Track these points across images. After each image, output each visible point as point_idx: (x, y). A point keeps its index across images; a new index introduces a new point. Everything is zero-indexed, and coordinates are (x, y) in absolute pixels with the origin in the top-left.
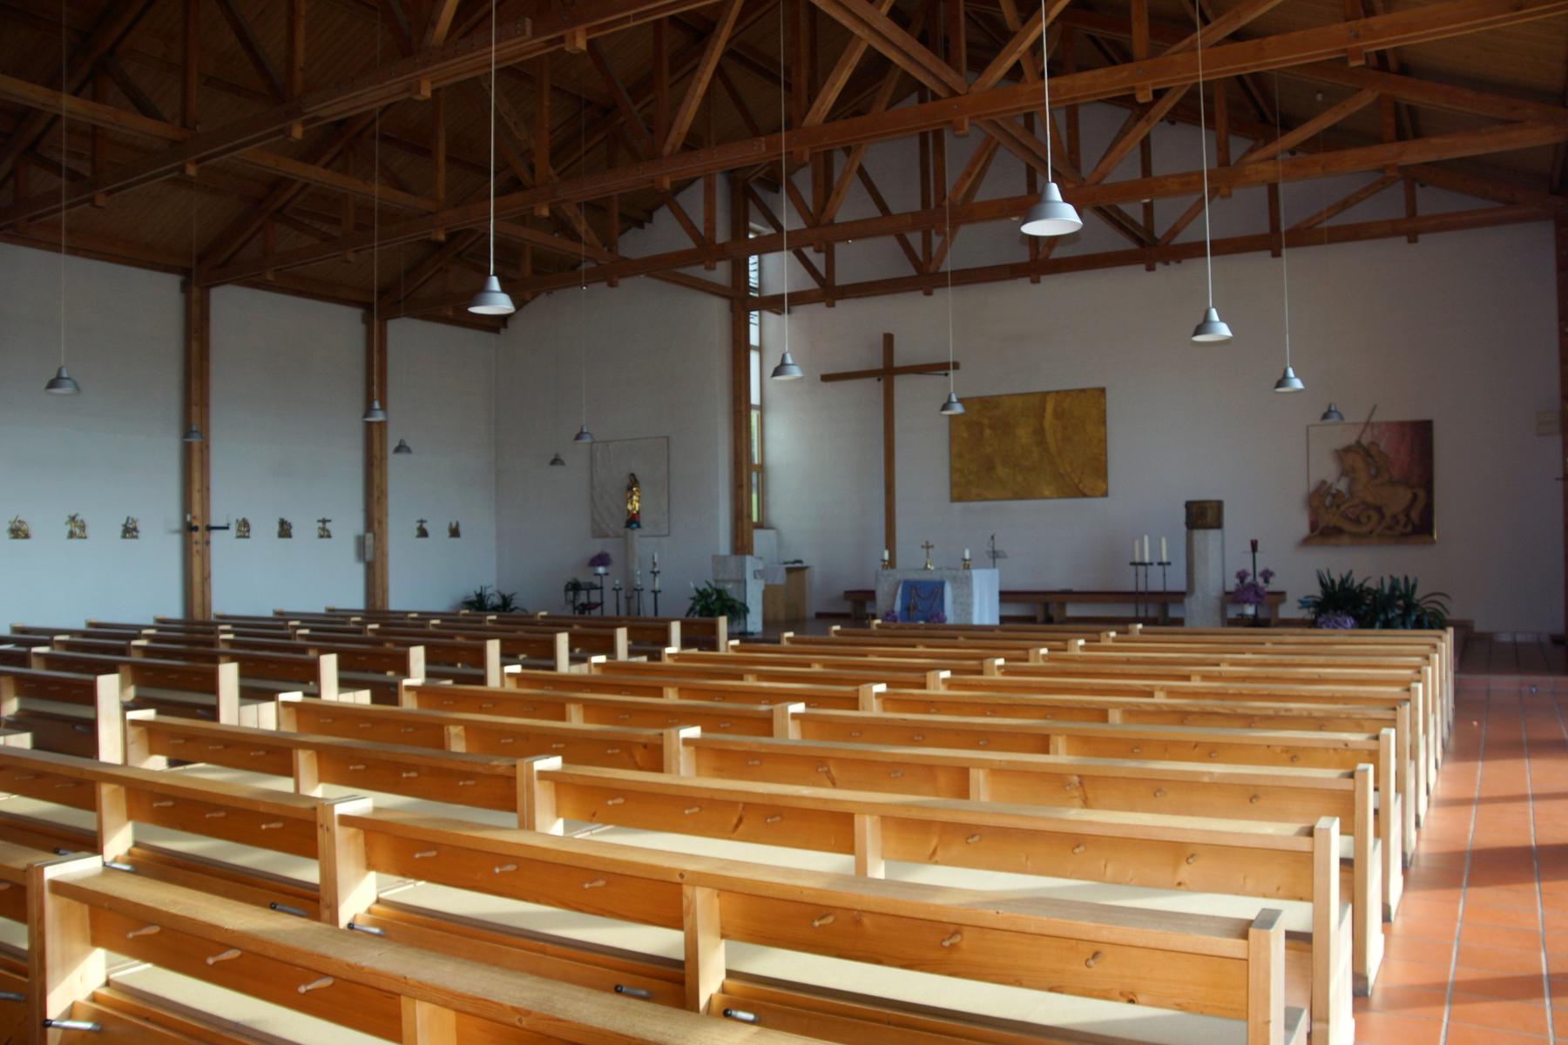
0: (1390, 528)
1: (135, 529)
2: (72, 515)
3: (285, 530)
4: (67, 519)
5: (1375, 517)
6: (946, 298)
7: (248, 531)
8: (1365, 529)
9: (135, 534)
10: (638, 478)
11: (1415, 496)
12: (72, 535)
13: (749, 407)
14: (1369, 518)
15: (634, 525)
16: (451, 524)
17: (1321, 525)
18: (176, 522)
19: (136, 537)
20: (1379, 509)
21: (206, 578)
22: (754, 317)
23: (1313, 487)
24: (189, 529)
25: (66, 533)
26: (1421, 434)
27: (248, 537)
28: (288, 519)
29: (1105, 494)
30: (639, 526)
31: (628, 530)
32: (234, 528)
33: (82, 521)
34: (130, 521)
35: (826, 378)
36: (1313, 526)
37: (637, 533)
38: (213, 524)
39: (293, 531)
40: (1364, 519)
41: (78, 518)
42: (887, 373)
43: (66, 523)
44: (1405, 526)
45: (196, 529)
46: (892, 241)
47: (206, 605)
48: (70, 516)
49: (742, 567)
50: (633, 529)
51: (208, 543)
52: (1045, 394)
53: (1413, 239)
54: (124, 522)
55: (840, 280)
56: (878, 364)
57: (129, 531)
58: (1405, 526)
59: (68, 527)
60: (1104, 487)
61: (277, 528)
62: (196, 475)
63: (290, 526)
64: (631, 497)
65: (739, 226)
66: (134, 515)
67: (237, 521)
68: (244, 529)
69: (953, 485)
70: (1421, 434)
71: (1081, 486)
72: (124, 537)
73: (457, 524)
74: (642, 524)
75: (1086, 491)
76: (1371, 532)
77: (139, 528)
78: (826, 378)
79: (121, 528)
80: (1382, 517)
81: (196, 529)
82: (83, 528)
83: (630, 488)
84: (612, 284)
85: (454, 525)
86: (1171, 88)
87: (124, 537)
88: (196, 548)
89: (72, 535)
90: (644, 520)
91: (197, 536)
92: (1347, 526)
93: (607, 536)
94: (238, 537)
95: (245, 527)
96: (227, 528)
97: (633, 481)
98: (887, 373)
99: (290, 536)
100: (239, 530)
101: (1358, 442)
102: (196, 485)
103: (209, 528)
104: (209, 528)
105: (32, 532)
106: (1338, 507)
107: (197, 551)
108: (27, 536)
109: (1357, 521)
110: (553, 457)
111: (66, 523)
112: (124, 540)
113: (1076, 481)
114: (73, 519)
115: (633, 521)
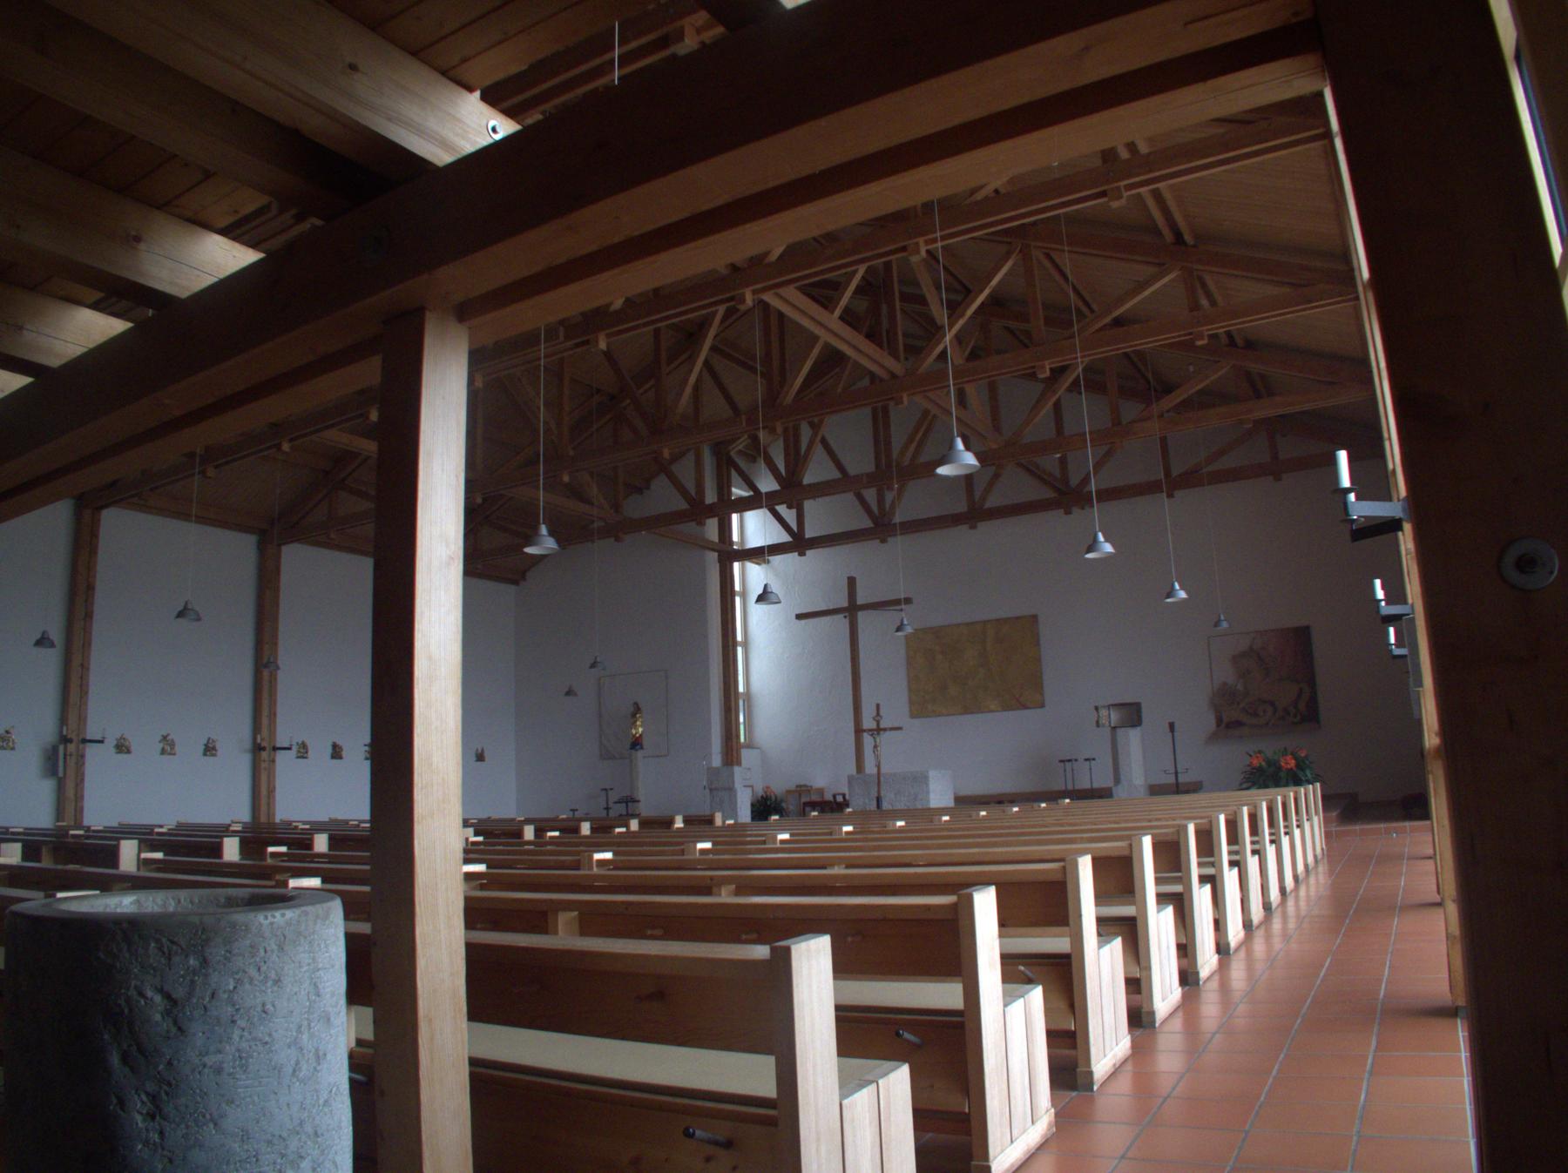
1: (214, 748)
2: (165, 734)
3: (337, 753)
4: (160, 738)
6: (898, 543)
7: (307, 752)
9: (214, 752)
10: (640, 706)
11: (1301, 689)
12: (163, 752)
13: (735, 643)
14: (1264, 711)
15: (638, 747)
16: (477, 750)
17: (1225, 720)
18: (248, 744)
19: (214, 755)
20: (1272, 704)
21: (271, 791)
22: (736, 566)
24: (257, 749)
25: (159, 750)
26: (1301, 638)
27: (306, 758)
28: (339, 742)
29: (1042, 706)
30: (642, 748)
31: (633, 751)
32: (295, 748)
33: (173, 741)
34: (211, 741)
35: (799, 617)
36: (1219, 721)
37: (640, 754)
38: (278, 745)
39: (344, 754)
41: (169, 738)
43: (160, 742)
44: (1295, 716)
45: (264, 749)
46: (849, 497)
47: (271, 814)
48: (163, 736)
49: (732, 775)
50: (637, 750)
51: (273, 761)
52: (985, 622)
53: (1278, 479)
54: (206, 742)
55: (809, 533)
57: (210, 749)
58: (1295, 716)
59: (161, 745)
61: (329, 750)
62: (265, 702)
63: (341, 748)
64: (636, 722)
65: (723, 488)
66: (214, 737)
67: (297, 743)
68: (303, 752)
69: (911, 702)
70: (1301, 638)
72: (205, 754)
73: (483, 750)
77: (217, 748)
78: (799, 617)
79: (203, 747)
81: (264, 749)
82: (172, 744)
83: (634, 715)
84: (617, 539)
86: (1070, 365)
87: (205, 754)
88: (263, 765)
89: (163, 752)
90: (645, 742)
91: (264, 755)
94: (298, 757)
95: (304, 748)
96: (289, 749)
97: (637, 709)
99: (341, 758)
100: (299, 752)
102: (265, 712)
103: (275, 749)
104: (275, 749)
105: (133, 748)
106: (1238, 704)
107: (265, 769)
108: (129, 752)
109: (1255, 714)
110: (567, 690)
111: (160, 742)
112: (205, 758)
114: (165, 738)
115: (636, 744)
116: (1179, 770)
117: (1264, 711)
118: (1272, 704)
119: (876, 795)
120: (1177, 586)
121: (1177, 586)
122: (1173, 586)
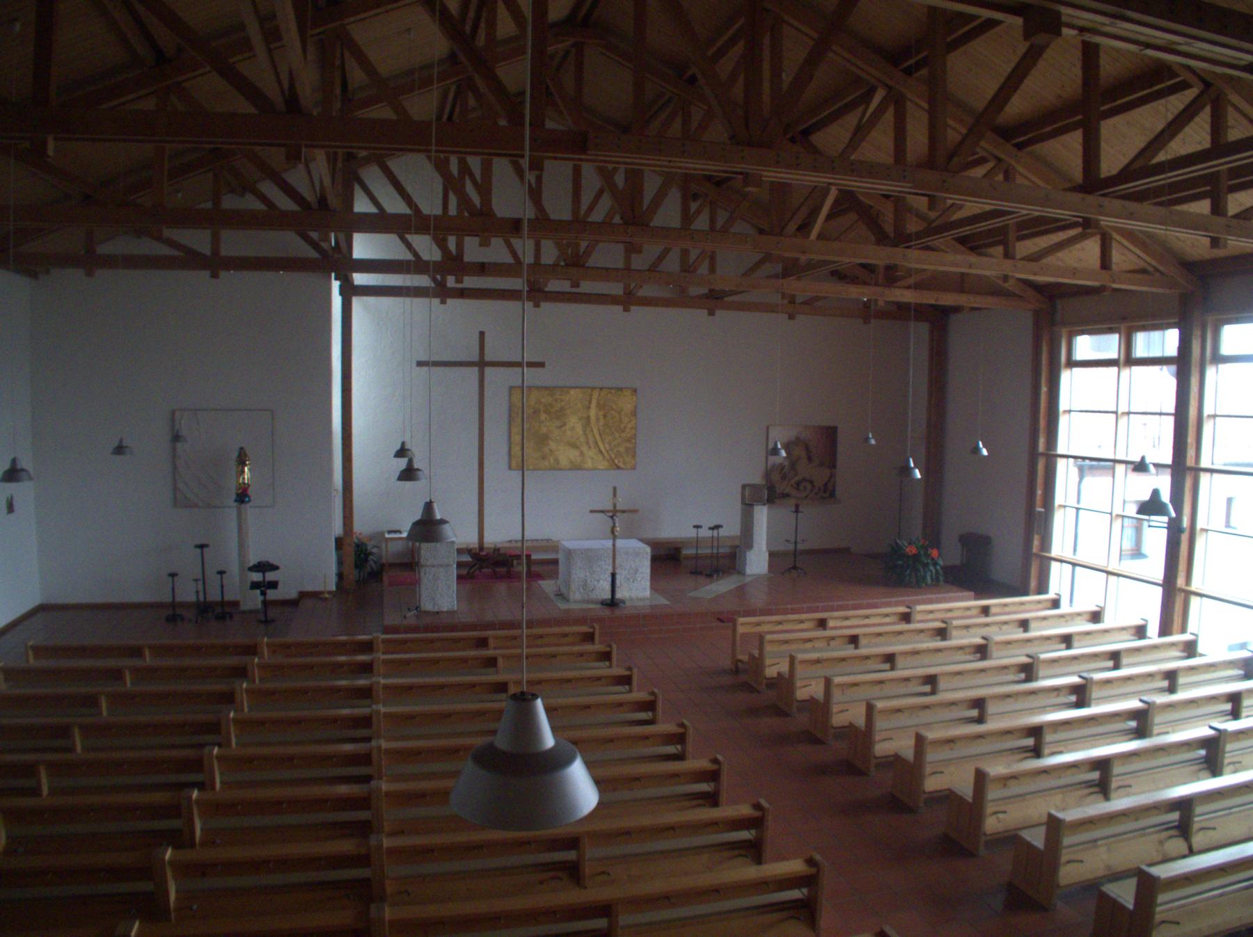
0: (816, 494)
5: (809, 487)
8: (804, 494)
10: (247, 452)
14: (805, 488)
15: (247, 499)
20: (811, 482)
23: (769, 467)
26: (830, 434)
29: (634, 468)
31: (243, 505)
35: (420, 364)
40: (801, 488)
42: (482, 364)
52: (593, 388)
53: (866, 320)
56: (476, 358)
58: (825, 491)
60: (633, 462)
70: (830, 434)
71: (616, 461)
74: (252, 498)
75: (621, 465)
76: (806, 497)
78: (420, 364)
80: (813, 486)
85: (10, 498)
90: (250, 491)
92: (794, 493)
93: (196, 506)
98: (482, 364)
101: (798, 439)
113: (613, 456)
115: (242, 496)
116: (798, 540)
117: (805, 488)
118: (811, 482)
119: (610, 570)
120: (981, 445)
121: (981, 445)
122: (978, 444)
